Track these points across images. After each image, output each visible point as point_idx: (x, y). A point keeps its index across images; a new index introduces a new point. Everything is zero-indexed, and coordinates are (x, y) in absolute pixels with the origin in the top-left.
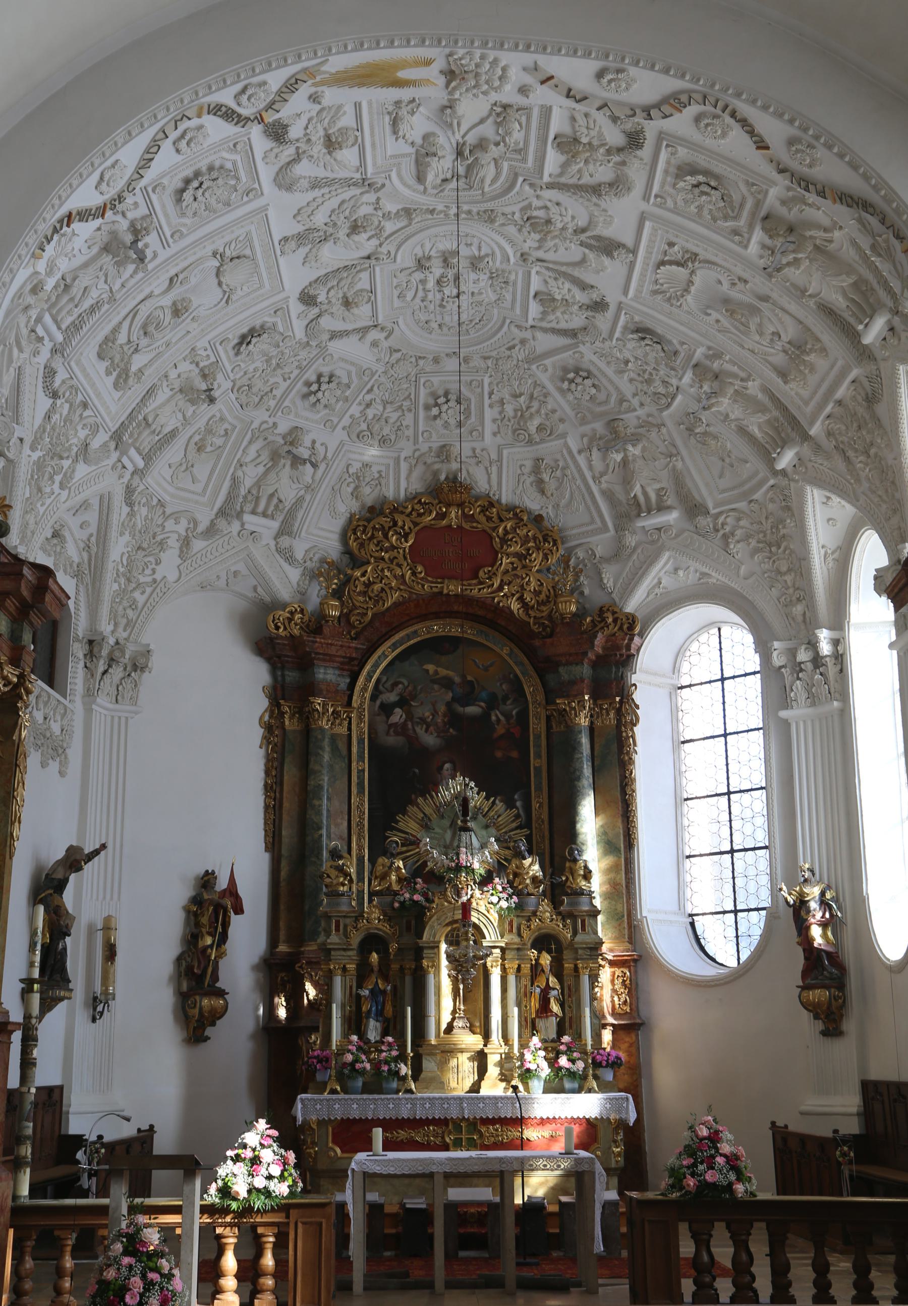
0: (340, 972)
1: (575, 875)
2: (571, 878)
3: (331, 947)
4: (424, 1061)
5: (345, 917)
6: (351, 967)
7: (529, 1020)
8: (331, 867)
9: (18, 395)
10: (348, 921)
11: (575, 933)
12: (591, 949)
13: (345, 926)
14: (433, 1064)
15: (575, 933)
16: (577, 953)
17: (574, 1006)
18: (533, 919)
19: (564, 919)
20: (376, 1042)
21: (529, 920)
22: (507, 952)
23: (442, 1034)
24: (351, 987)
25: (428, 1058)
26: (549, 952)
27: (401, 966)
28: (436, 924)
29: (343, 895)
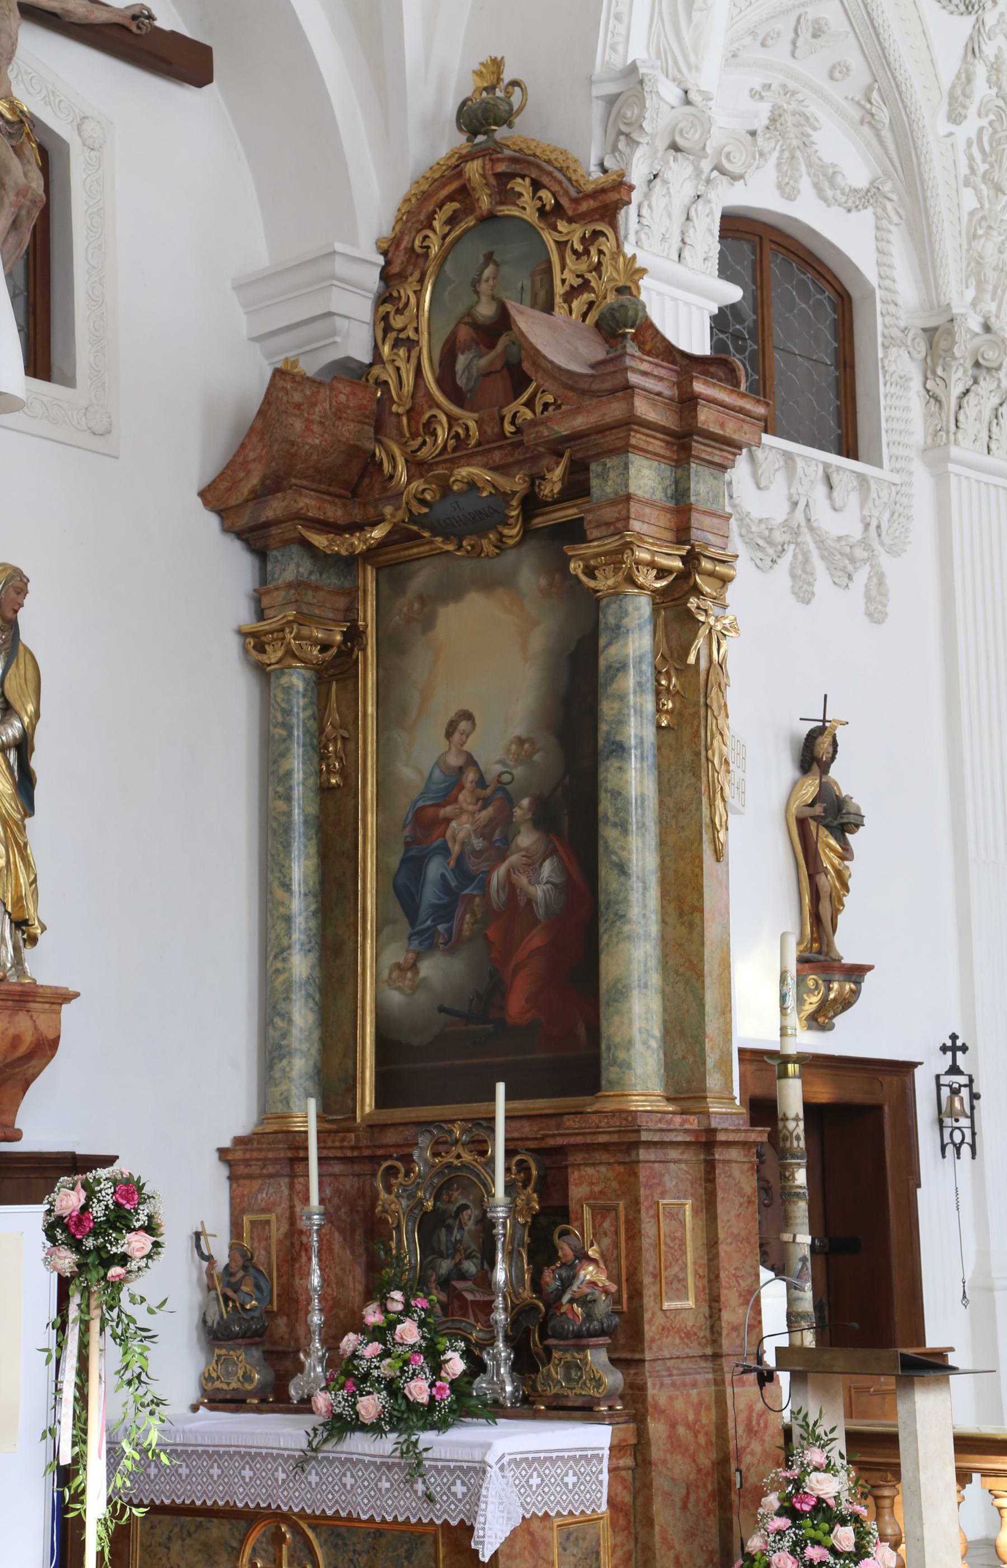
9: (877, 35)
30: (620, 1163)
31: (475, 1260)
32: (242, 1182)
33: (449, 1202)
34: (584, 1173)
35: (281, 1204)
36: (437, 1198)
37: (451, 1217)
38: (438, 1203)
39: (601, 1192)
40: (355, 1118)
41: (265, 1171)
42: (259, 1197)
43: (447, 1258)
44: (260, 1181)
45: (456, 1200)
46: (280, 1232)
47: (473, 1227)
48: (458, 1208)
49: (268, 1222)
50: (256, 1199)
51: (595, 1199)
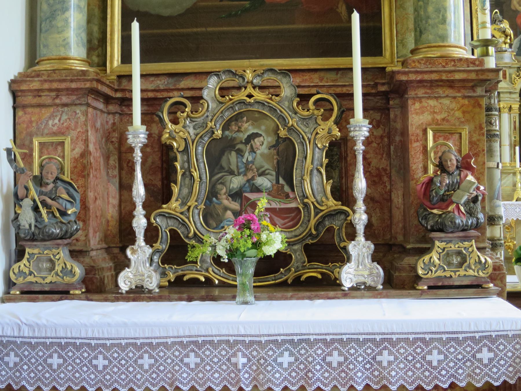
0: (507, 110)
5: (510, 67)
8: (495, 29)
10: (512, 71)
13: (510, 75)
24: (515, 122)
29: (506, 51)
30: (464, 97)
31: (268, 176)
32: (30, 110)
33: (239, 131)
34: (426, 105)
35: (76, 127)
36: (226, 127)
37: (241, 142)
38: (227, 133)
39: (443, 119)
40: (106, 70)
41: (58, 101)
42: (50, 122)
43: (239, 174)
44: (52, 109)
45: (246, 130)
46: (74, 152)
47: (266, 151)
48: (248, 136)
49: (62, 144)
50: (47, 124)
51: (437, 124)
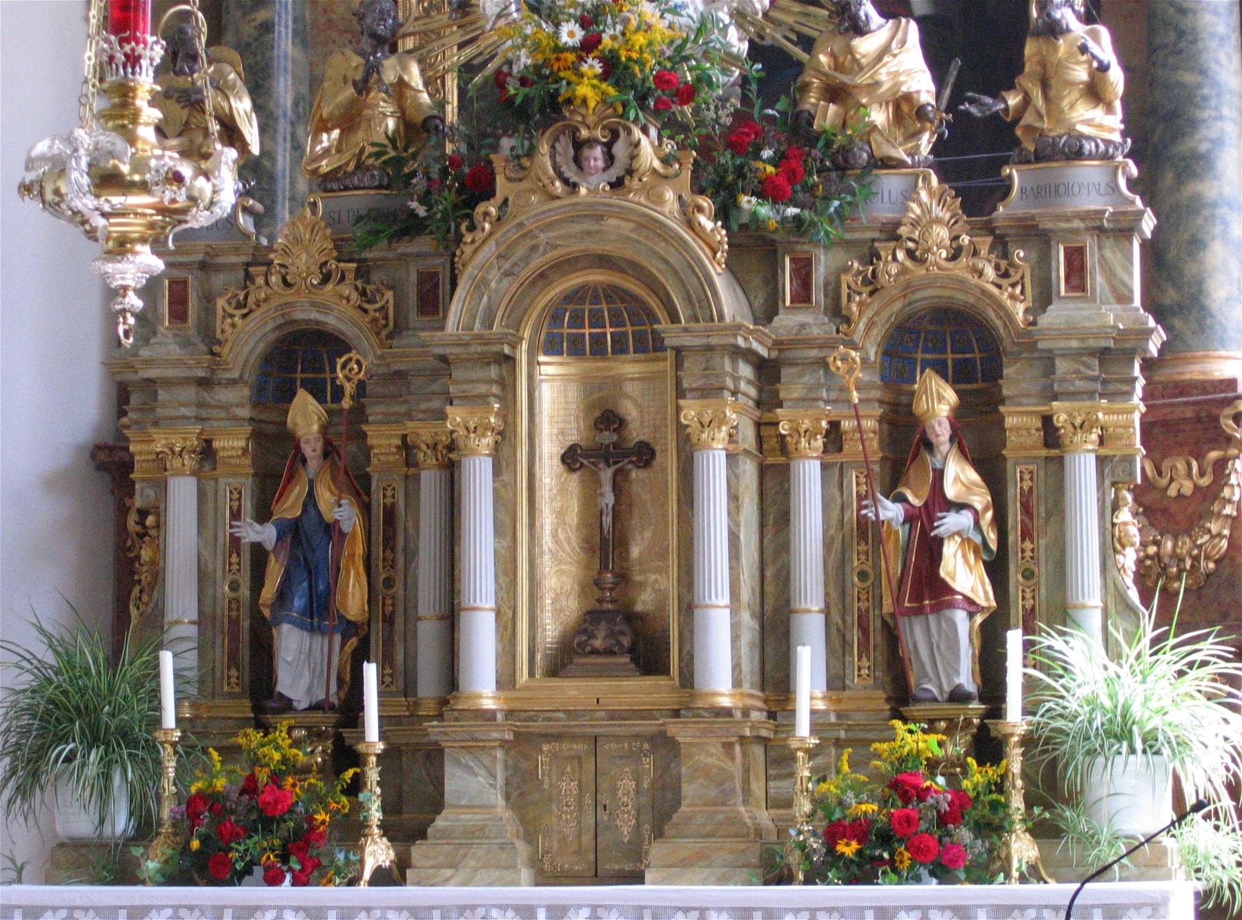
0: (189, 462)
1: (1053, 82)
2: (1039, 101)
3: (153, 373)
4: (449, 769)
6: (232, 444)
7: (875, 625)
11: (1044, 298)
12: (1103, 354)
13: (208, 299)
14: (482, 779)
15: (1044, 298)
16: (1049, 369)
17: (1043, 571)
18: (884, 249)
19: (1001, 246)
20: (311, 708)
21: (872, 257)
22: (786, 372)
23: (523, 676)
25: (467, 759)
26: (958, 376)
27: (404, 437)
28: (494, 276)
